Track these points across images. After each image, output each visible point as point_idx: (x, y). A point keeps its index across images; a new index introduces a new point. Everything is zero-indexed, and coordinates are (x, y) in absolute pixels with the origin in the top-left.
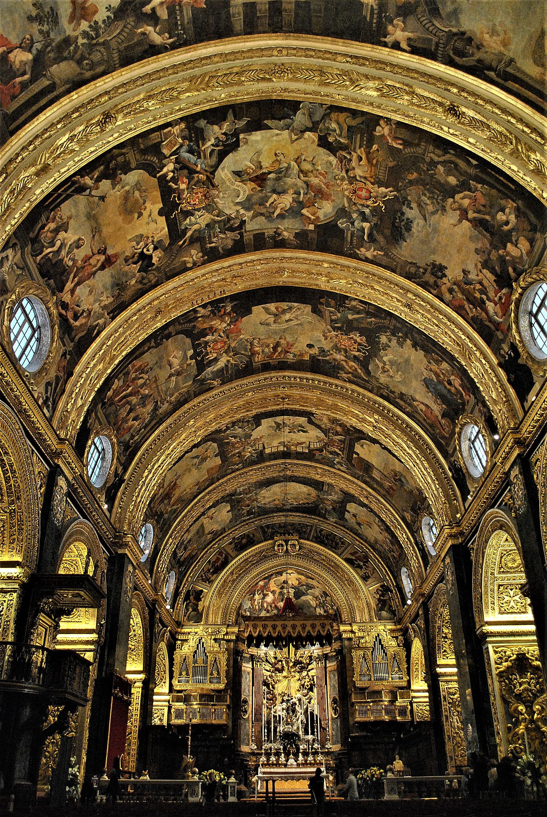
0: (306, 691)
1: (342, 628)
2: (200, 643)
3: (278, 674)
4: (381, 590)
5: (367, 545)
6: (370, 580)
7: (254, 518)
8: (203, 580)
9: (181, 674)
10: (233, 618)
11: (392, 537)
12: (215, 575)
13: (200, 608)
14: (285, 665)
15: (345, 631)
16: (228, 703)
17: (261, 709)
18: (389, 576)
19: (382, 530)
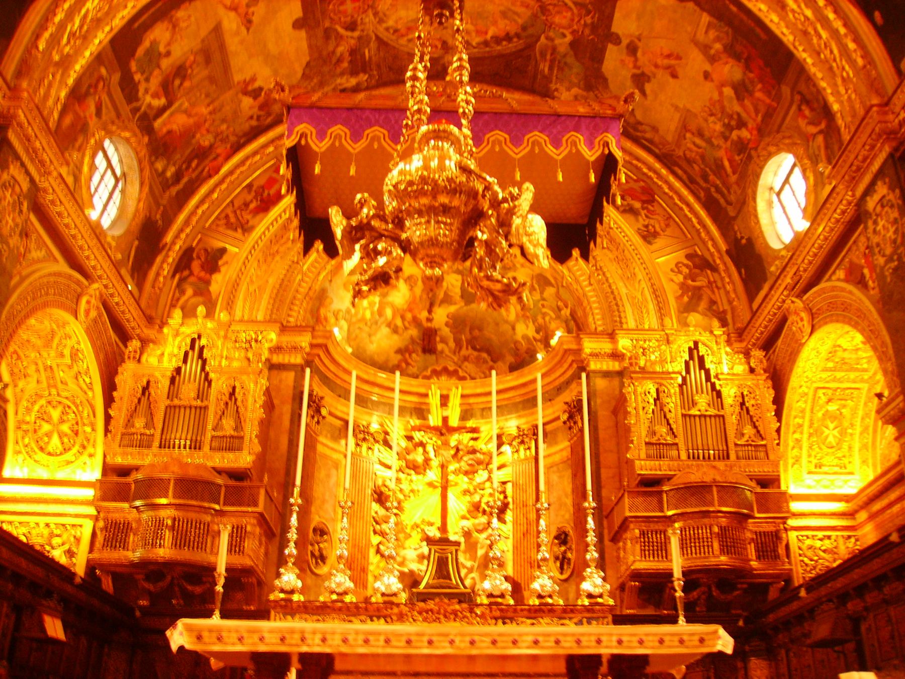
0: (483, 519)
1: (589, 345)
2: (192, 347)
3: (414, 476)
4: (687, 266)
5: (650, 159)
6: (659, 242)
7: (367, 88)
8: (229, 225)
9: (129, 423)
10: (297, 315)
11: (748, 67)
12: (261, 215)
13: (214, 288)
14: (432, 454)
15: (595, 355)
16: (260, 509)
17: (365, 557)
18: (708, 232)
19: (712, 59)
